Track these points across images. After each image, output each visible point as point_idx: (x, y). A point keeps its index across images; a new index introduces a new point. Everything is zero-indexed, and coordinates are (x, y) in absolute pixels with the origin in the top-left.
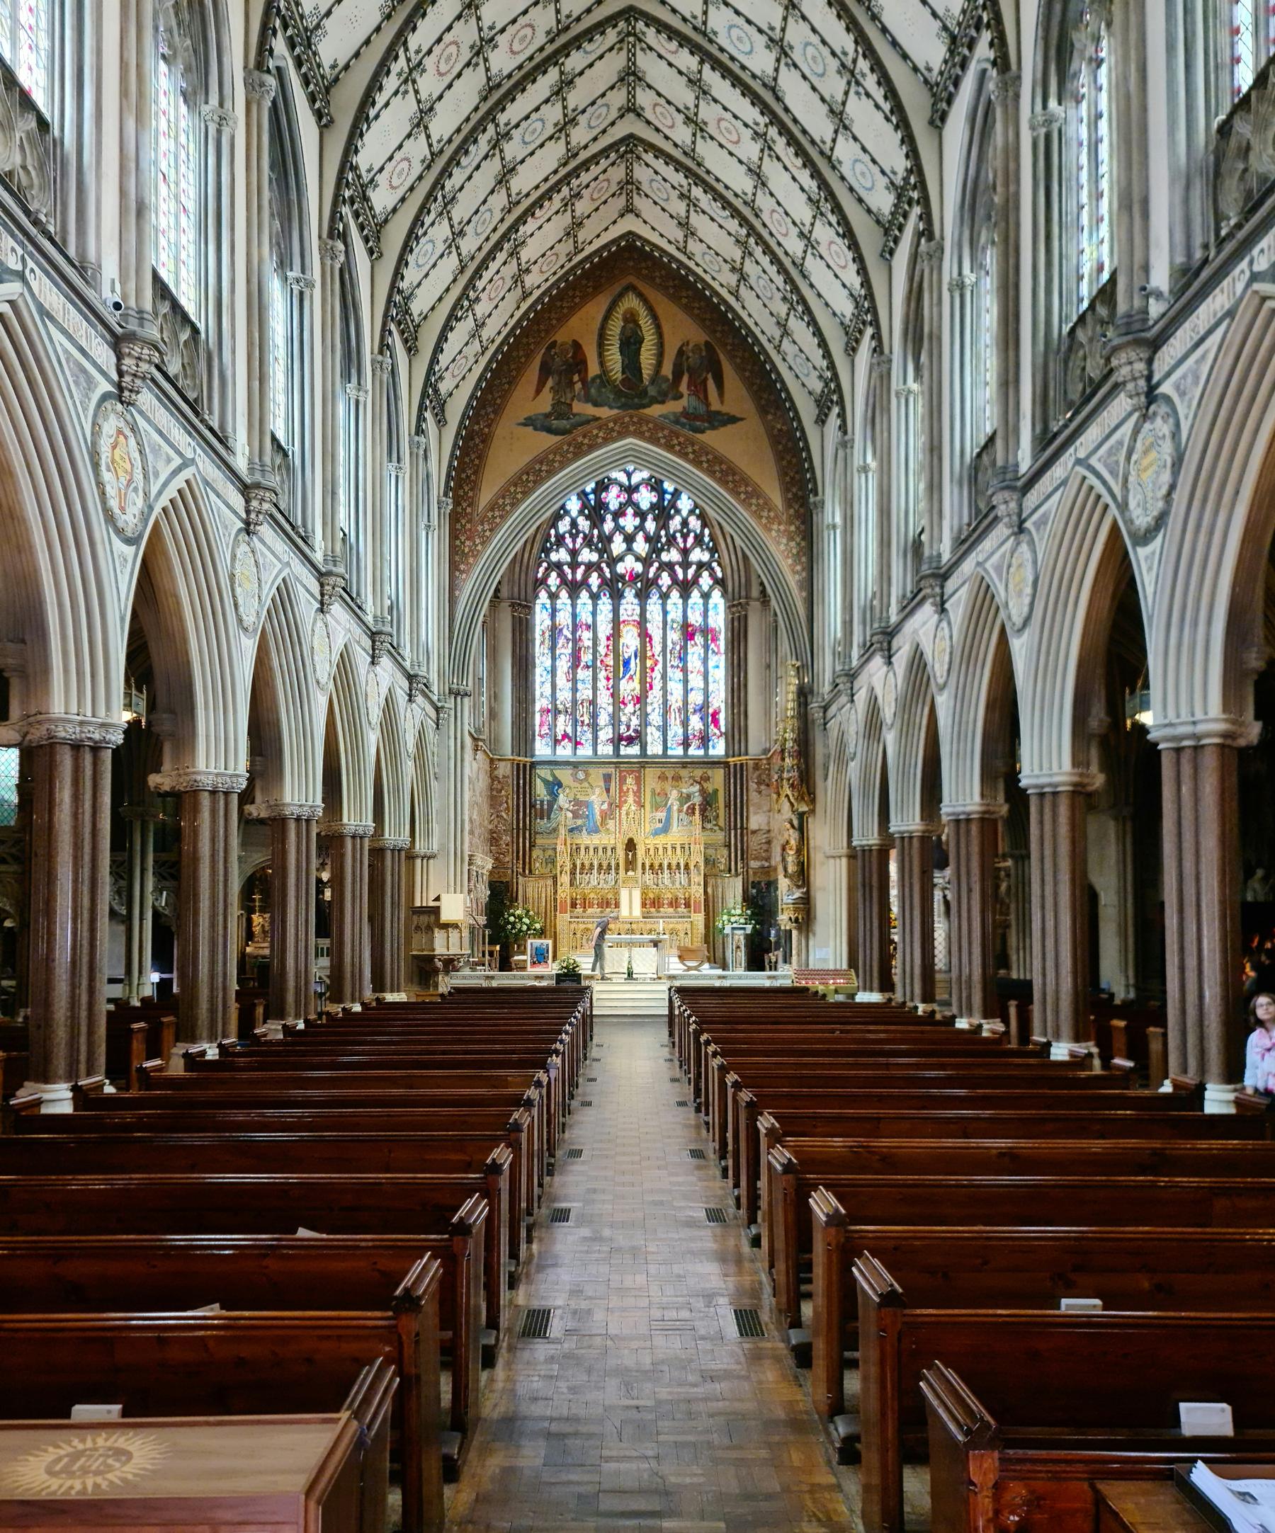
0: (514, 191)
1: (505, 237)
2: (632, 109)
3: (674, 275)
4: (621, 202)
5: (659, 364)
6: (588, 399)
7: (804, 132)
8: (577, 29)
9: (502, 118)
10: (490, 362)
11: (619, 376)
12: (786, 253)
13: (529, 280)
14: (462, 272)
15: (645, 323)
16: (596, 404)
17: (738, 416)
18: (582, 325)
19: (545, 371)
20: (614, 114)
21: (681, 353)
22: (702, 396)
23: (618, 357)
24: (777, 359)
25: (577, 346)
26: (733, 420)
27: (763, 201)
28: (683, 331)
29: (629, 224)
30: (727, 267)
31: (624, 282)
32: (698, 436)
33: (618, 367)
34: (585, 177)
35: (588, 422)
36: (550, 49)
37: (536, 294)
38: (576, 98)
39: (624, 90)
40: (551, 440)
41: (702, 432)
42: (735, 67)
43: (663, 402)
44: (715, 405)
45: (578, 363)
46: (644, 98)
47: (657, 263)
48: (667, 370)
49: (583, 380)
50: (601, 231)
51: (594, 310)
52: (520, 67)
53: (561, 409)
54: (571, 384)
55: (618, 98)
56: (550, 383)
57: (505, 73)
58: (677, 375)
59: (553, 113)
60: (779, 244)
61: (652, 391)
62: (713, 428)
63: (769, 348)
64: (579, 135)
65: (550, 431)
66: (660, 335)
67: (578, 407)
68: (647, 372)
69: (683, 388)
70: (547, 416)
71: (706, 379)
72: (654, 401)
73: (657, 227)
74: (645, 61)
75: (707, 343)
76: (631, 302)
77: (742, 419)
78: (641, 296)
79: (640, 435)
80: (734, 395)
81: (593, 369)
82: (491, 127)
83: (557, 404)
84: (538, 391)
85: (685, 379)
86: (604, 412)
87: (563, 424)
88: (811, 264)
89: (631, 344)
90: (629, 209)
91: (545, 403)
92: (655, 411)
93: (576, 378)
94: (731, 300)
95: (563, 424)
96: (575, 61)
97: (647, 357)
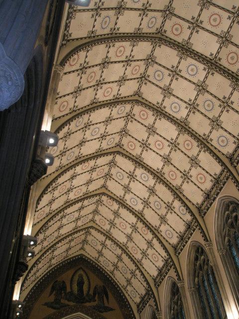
0: (60, 233)
1: (52, 246)
2: (93, 220)
3: (94, 266)
4: (80, 246)
5: (89, 290)
6: (66, 299)
7: (150, 224)
8: (90, 194)
9: (66, 211)
10: (36, 284)
11: (76, 292)
12: (135, 259)
13: (54, 262)
14: (41, 251)
15: (85, 278)
16: (69, 301)
17: (113, 308)
18: (66, 276)
19: (53, 288)
20: (88, 221)
21: (95, 288)
22: (102, 300)
23: (76, 287)
24: (125, 292)
25: (64, 282)
26: (112, 310)
27: (130, 245)
28: (96, 282)
29: (82, 252)
30: (111, 265)
31: (79, 267)
32: (100, 313)
33: (76, 289)
34: (76, 235)
35: (66, 306)
36: (83, 197)
37: (53, 266)
38: (83, 213)
39: (92, 215)
40: (53, 311)
41: (102, 312)
42: (131, 208)
43: (90, 302)
44: (106, 305)
45: (64, 288)
46: (97, 218)
47: (89, 263)
48: (91, 292)
49: (65, 293)
50: (74, 252)
51: (70, 273)
52: (75, 199)
53: (57, 301)
54: (61, 293)
55: (91, 217)
56: (54, 292)
57: (71, 199)
58: (94, 294)
59: (76, 215)
60: (133, 256)
61: (87, 298)
62: (106, 312)
63: (122, 289)
64: (80, 223)
65: (54, 308)
66: (89, 282)
67: (62, 301)
68: (85, 292)
69: (96, 298)
70: (52, 303)
71: (103, 296)
72: (87, 301)
73: (90, 253)
74: (101, 209)
75: (103, 286)
76: (81, 272)
77: (115, 310)
78: (84, 271)
79: (81, 312)
80: (112, 302)
81: (68, 290)
82: (62, 213)
83: (56, 300)
84: (50, 295)
85: (97, 295)
86: (71, 304)
87: (58, 306)
88: (144, 261)
89: (80, 284)
90: (82, 248)
91: (52, 298)
92: (88, 304)
93: (63, 292)
94: (111, 275)
95: (58, 306)
96: (86, 202)
97: (85, 288)
